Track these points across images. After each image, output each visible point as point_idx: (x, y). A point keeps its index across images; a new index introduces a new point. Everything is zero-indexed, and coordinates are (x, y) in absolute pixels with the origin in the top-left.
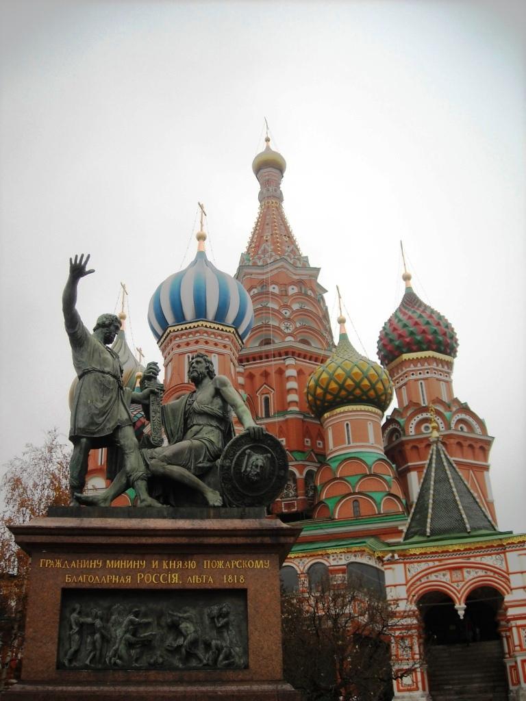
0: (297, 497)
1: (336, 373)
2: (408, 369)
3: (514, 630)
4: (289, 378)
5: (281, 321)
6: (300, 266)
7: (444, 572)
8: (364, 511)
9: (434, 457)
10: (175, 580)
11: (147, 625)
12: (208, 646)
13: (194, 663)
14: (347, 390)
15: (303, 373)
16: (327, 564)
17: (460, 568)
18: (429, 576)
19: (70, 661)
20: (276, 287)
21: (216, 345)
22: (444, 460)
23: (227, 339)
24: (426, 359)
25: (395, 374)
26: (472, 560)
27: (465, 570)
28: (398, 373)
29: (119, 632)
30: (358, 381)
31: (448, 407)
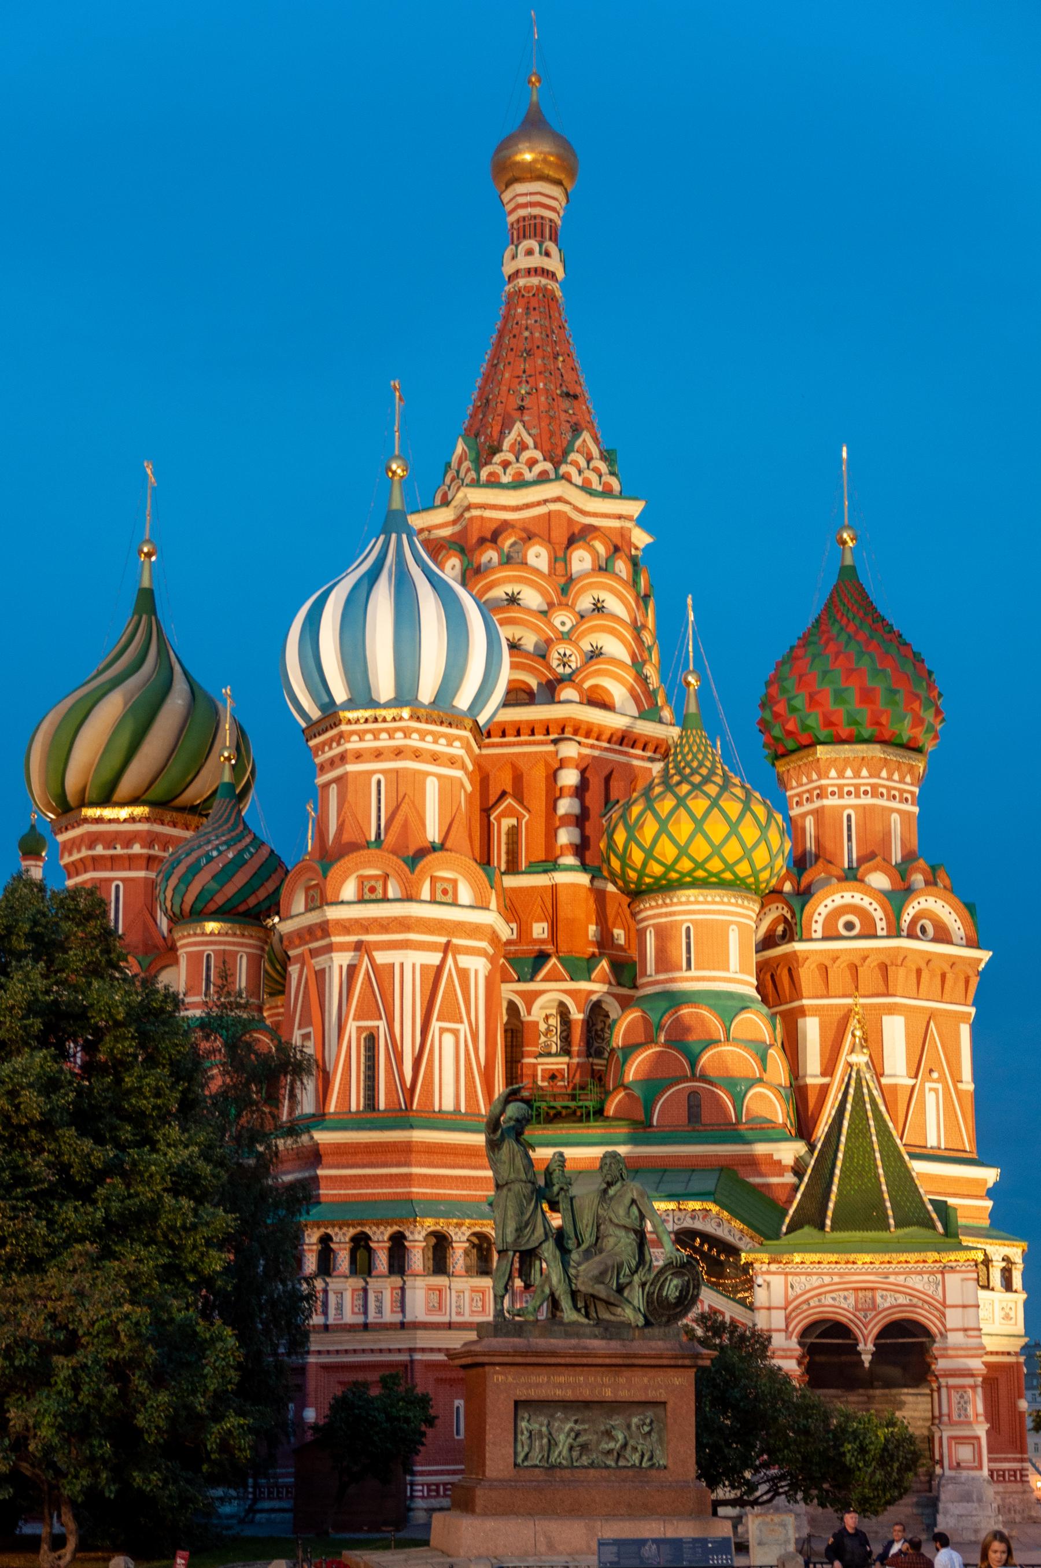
2: (824, 782)
3: (944, 1391)
6: (600, 488)
7: (846, 1293)
10: (608, 1394)
11: (585, 1430)
12: (635, 1449)
14: (692, 859)
17: (872, 1289)
18: (823, 1297)
19: (523, 1461)
21: (435, 758)
22: (867, 1099)
23: (457, 744)
25: (794, 784)
26: (892, 1279)
27: (878, 1294)
29: (562, 1437)
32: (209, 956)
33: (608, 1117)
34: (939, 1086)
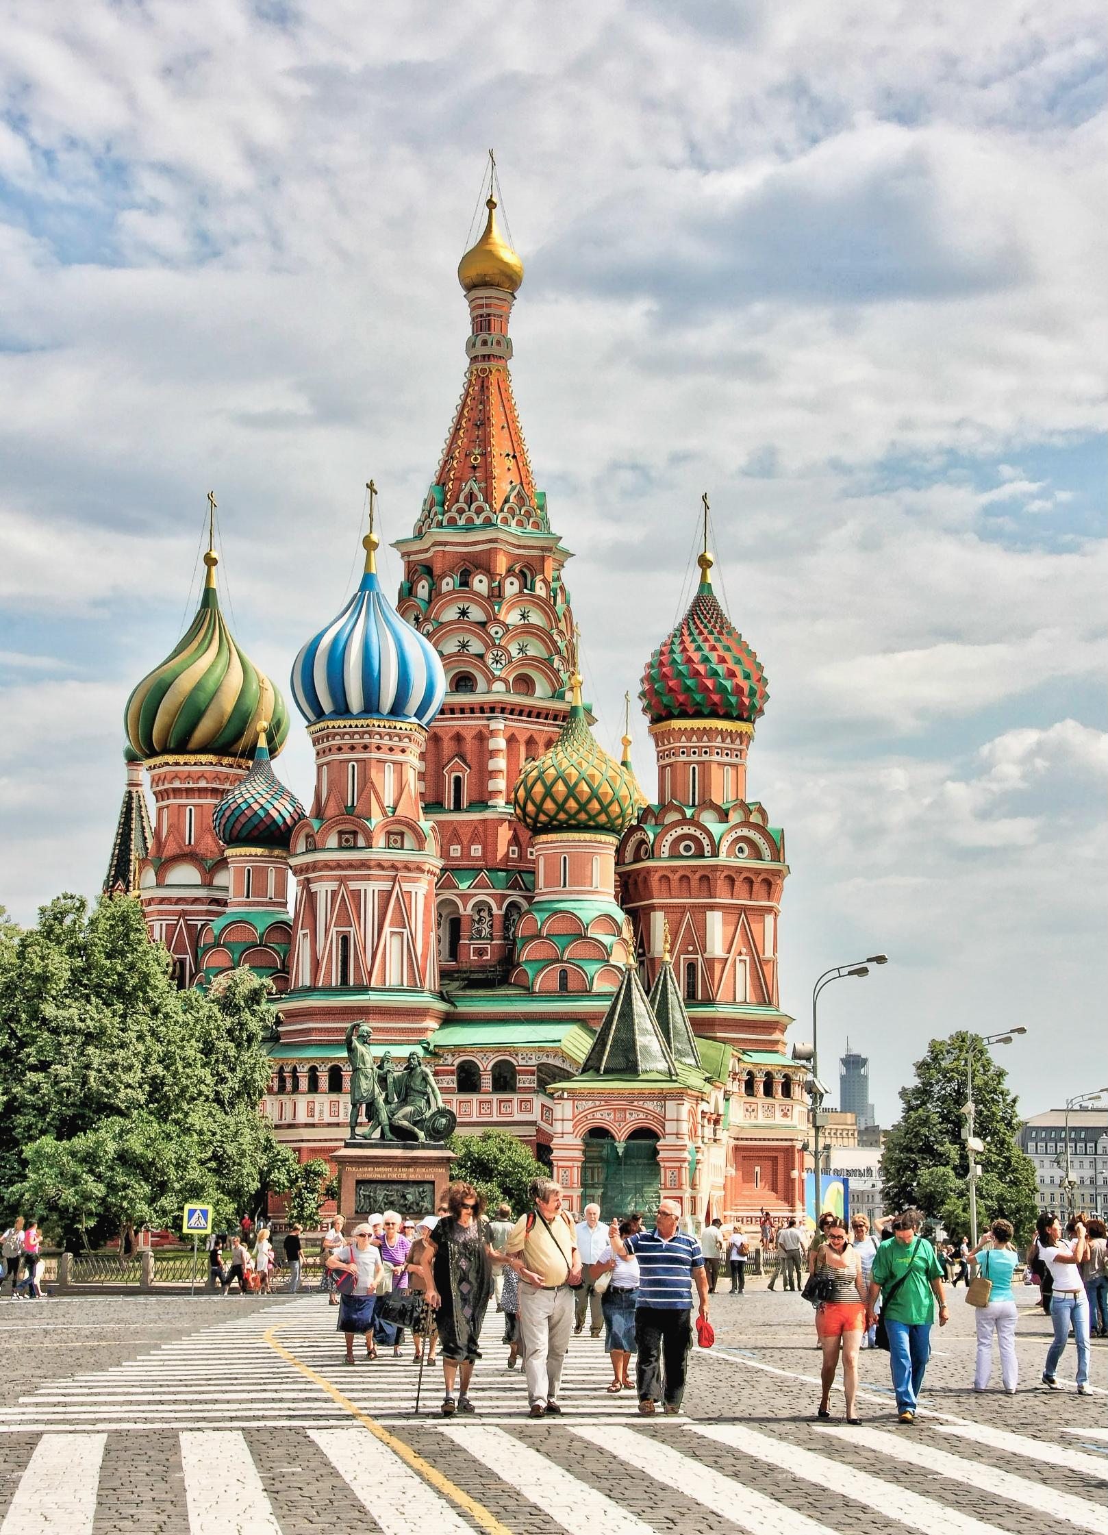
0: (492, 940)
1: (554, 789)
4: (493, 754)
5: (487, 647)
8: (572, 984)
9: (624, 987)
10: (404, 1177)
13: (411, 1211)
14: (566, 812)
15: (517, 741)
16: (516, 1064)
20: (484, 579)
21: (391, 750)
23: (406, 740)
24: (705, 731)
26: (635, 1103)
28: (663, 744)
29: (381, 1198)
30: (584, 799)
31: (723, 816)
32: (249, 870)
33: (511, 984)
34: (747, 959)
